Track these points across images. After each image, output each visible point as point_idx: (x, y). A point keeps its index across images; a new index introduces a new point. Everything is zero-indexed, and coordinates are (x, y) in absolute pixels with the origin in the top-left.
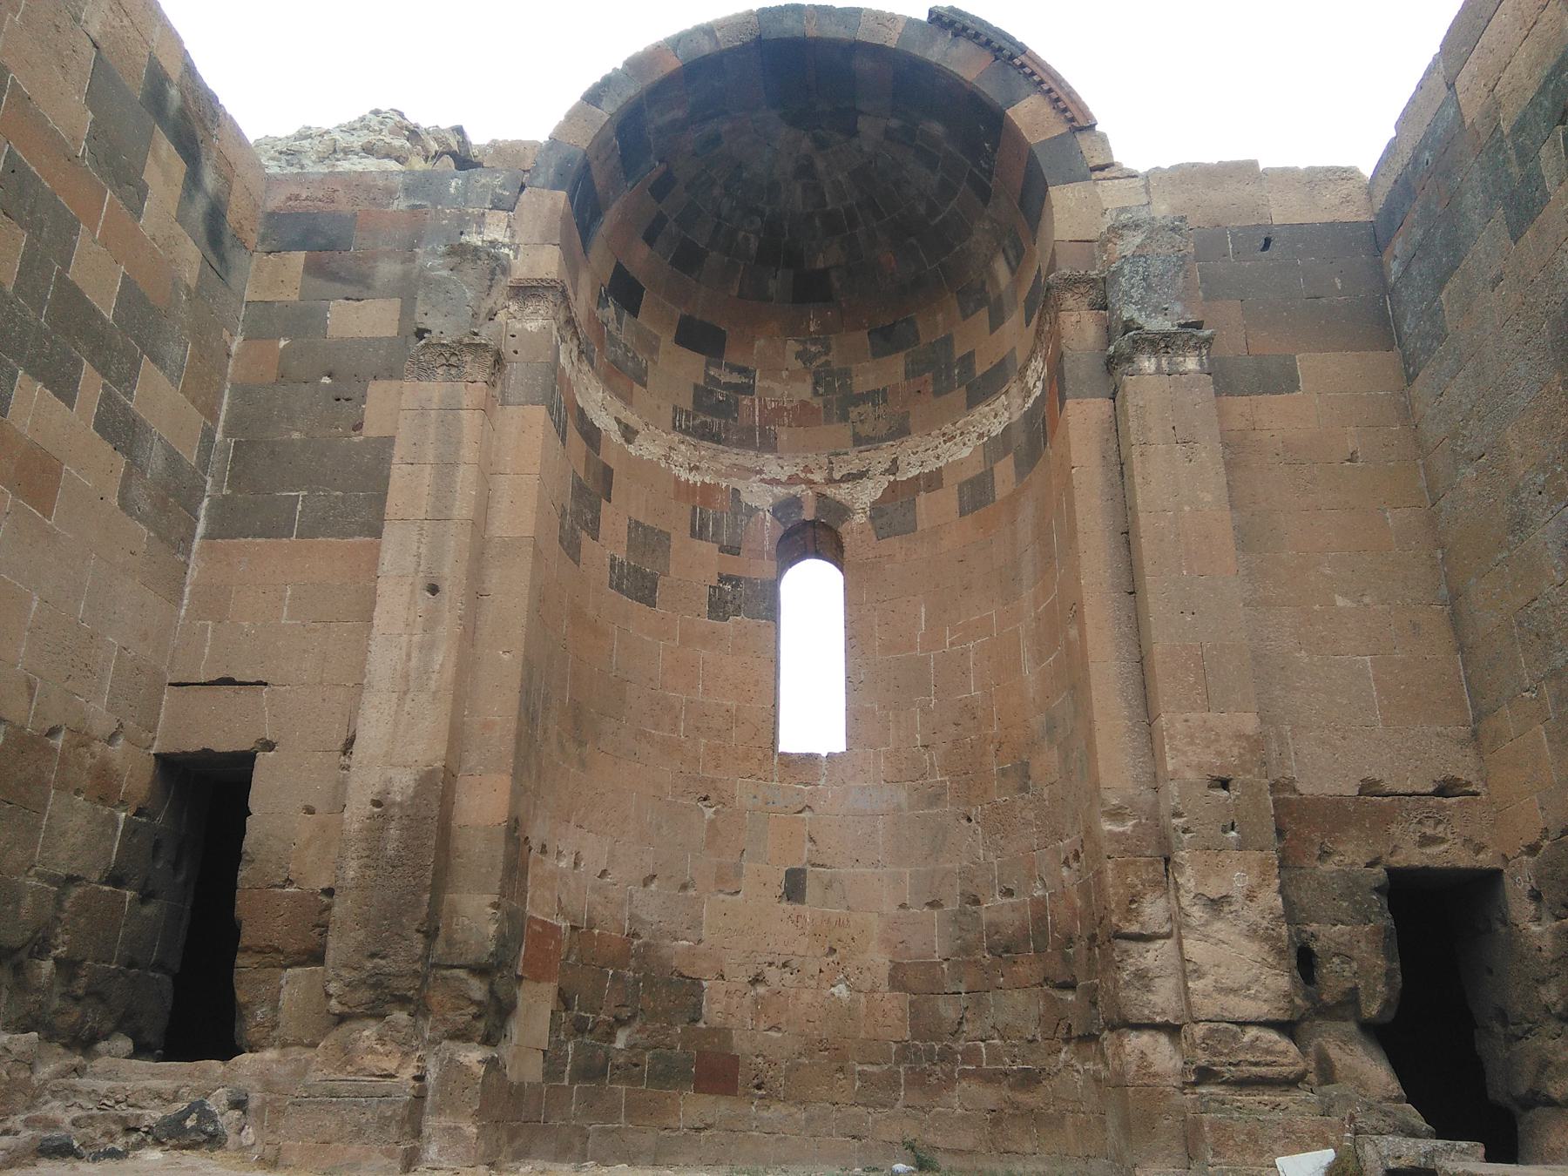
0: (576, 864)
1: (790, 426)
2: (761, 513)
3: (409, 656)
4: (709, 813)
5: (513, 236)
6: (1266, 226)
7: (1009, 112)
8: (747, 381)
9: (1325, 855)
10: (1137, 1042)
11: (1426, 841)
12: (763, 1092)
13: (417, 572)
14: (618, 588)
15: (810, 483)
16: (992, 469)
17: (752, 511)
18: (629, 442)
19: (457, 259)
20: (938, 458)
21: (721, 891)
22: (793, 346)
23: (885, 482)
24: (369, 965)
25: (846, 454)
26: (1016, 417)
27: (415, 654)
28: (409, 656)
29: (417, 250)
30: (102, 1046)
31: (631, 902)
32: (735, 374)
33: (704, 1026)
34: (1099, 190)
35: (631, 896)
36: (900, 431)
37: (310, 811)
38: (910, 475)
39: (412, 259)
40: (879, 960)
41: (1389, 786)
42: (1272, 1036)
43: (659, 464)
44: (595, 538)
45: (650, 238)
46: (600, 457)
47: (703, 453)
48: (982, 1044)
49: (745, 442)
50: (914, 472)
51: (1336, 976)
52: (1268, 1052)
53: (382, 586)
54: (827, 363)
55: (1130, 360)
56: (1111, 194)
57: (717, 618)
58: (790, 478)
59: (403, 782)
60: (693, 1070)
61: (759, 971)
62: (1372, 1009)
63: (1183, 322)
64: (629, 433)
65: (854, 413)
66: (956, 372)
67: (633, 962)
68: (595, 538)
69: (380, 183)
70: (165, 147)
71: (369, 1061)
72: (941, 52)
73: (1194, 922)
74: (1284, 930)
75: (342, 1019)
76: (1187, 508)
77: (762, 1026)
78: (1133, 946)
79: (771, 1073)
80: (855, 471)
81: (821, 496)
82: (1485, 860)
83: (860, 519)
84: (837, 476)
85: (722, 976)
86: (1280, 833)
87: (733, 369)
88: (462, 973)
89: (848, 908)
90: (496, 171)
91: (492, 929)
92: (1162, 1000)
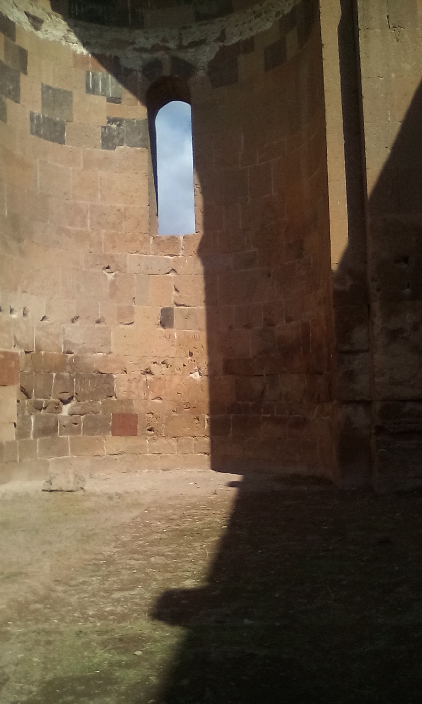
4: (110, 277)
12: (152, 433)
15: (167, 49)
18: (37, 29)
23: (217, 47)
25: (191, 27)
31: (64, 333)
33: (116, 399)
35: (64, 330)
43: (60, 43)
44: (17, 101)
46: (17, 43)
47: (92, 32)
50: (236, 40)
57: (108, 148)
60: (111, 423)
61: (147, 367)
67: (68, 368)
76: (393, 75)
77: (151, 397)
79: (157, 422)
80: (197, 40)
83: (201, 73)
84: (185, 43)
85: (125, 371)
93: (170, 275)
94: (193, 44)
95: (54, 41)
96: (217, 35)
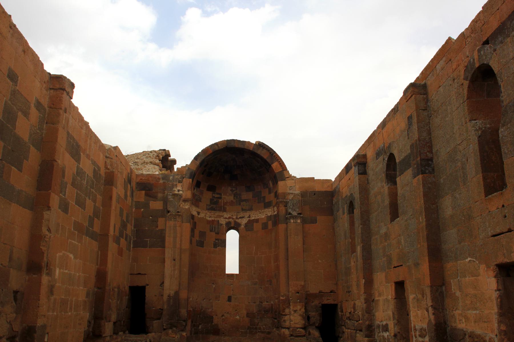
0: (193, 298)
1: (229, 206)
2: (223, 225)
3: (171, 272)
4: (214, 286)
5: (182, 188)
6: (315, 191)
7: (272, 165)
8: (220, 196)
9: (313, 302)
10: (283, 330)
11: (328, 299)
12: (224, 335)
13: (171, 257)
14: (197, 245)
15: (233, 218)
16: (268, 222)
17: (222, 225)
18: (199, 215)
19: (174, 196)
20: (258, 216)
21: (216, 300)
22: (230, 188)
24: (170, 321)
25: (240, 213)
26: (272, 214)
27: (172, 271)
28: (171, 272)
29: (165, 191)
30: (126, 332)
32: (218, 195)
34: (287, 182)
36: (251, 209)
37: (156, 296)
38: (253, 219)
39: (164, 193)
40: (245, 312)
41: (323, 291)
42: (301, 330)
43: (204, 217)
44: (194, 237)
45: (203, 174)
47: (212, 213)
48: (262, 327)
49: (220, 210)
50: (253, 218)
51: (312, 320)
52: (301, 332)
53: (166, 259)
54: (236, 192)
55: (289, 220)
56: (289, 182)
57: (215, 248)
58: (229, 217)
59: (172, 293)
62: (317, 325)
63: (298, 213)
64: (199, 213)
65: (242, 203)
66: (262, 199)
68: (194, 237)
69: (157, 177)
70: (129, 185)
71: (171, 335)
72: (260, 152)
73: (292, 313)
74: (304, 315)
75: (164, 329)
76: (296, 247)
78: (284, 316)
80: (242, 216)
81: (235, 222)
82: (335, 302)
83: (243, 226)
84: (238, 217)
86: (306, 299)
87: (218, 194)
88: (182, 321)
89: (239, 303)
90: (179, 175)
91: (186, 315)
92: (287, 324)
93: (231, 286)
94: (240, 218)
95: (202, 217)
96: (248, 216)
